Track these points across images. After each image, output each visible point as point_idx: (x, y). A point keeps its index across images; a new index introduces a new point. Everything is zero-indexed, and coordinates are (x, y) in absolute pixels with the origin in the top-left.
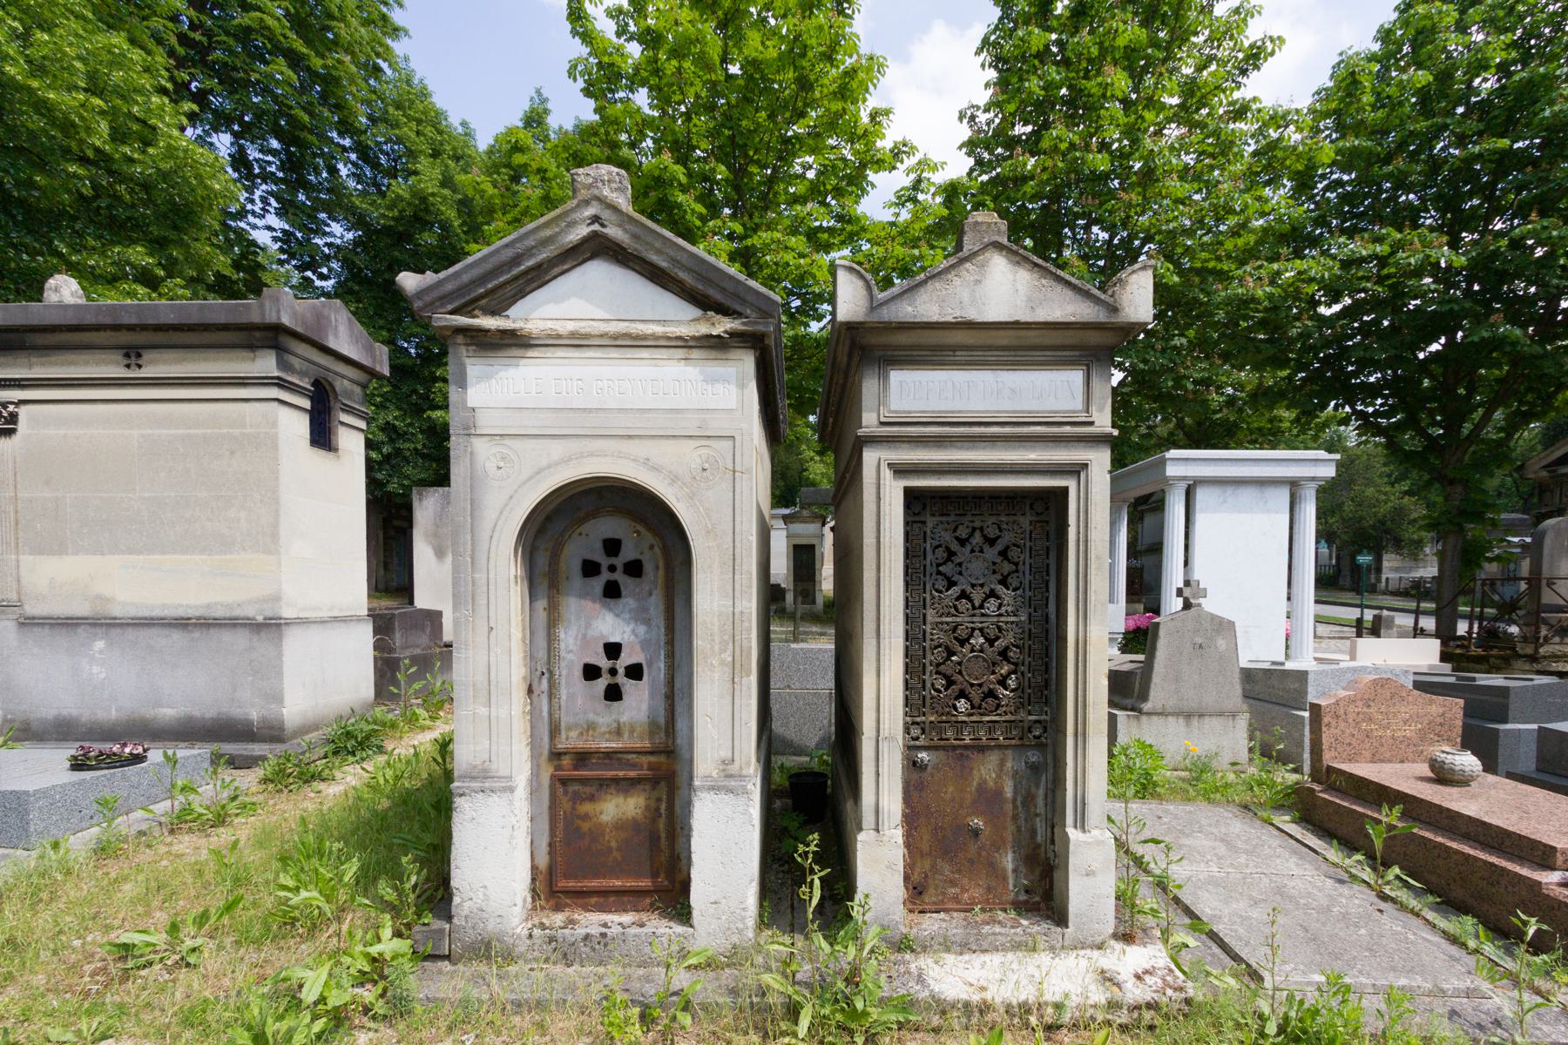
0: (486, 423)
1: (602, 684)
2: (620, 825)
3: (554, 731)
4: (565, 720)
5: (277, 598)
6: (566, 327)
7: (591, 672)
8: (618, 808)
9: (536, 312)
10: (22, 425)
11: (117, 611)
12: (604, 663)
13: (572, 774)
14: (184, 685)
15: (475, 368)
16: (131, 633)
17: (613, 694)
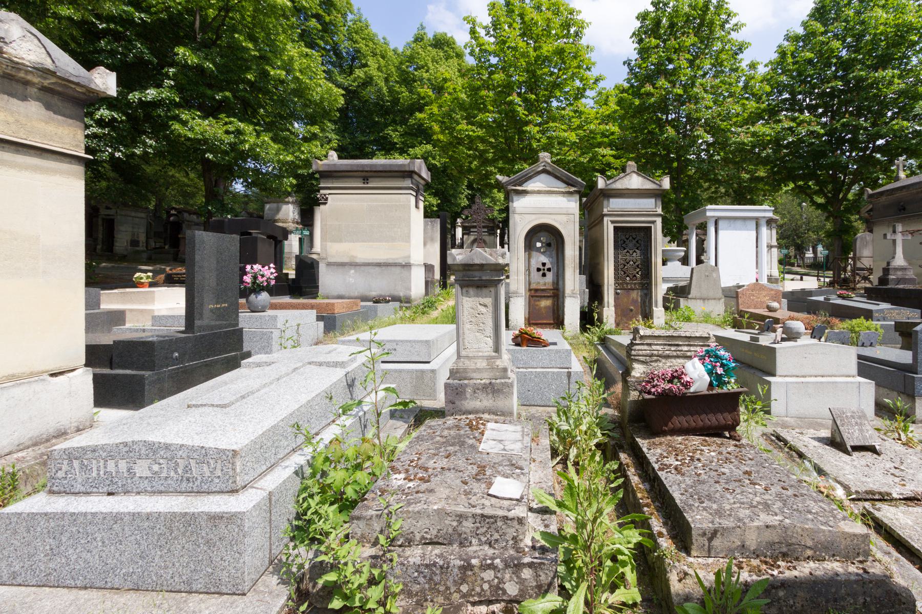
0: (518, 210)
1: (541, 272)
2: (546, 307)
3: (530, 284)
4: (532, 281)
5: (409, 257)
6: (536, 189)
7: (539, 270)
8: (545, 303)
9: (530, 186)
10: (329, 201)
11: (358, 261)
12: (542, 268)
13: (534, 294)
14: (379, 285)
15: (515, 198)
16: (363, 268)
17: (544, 275)
